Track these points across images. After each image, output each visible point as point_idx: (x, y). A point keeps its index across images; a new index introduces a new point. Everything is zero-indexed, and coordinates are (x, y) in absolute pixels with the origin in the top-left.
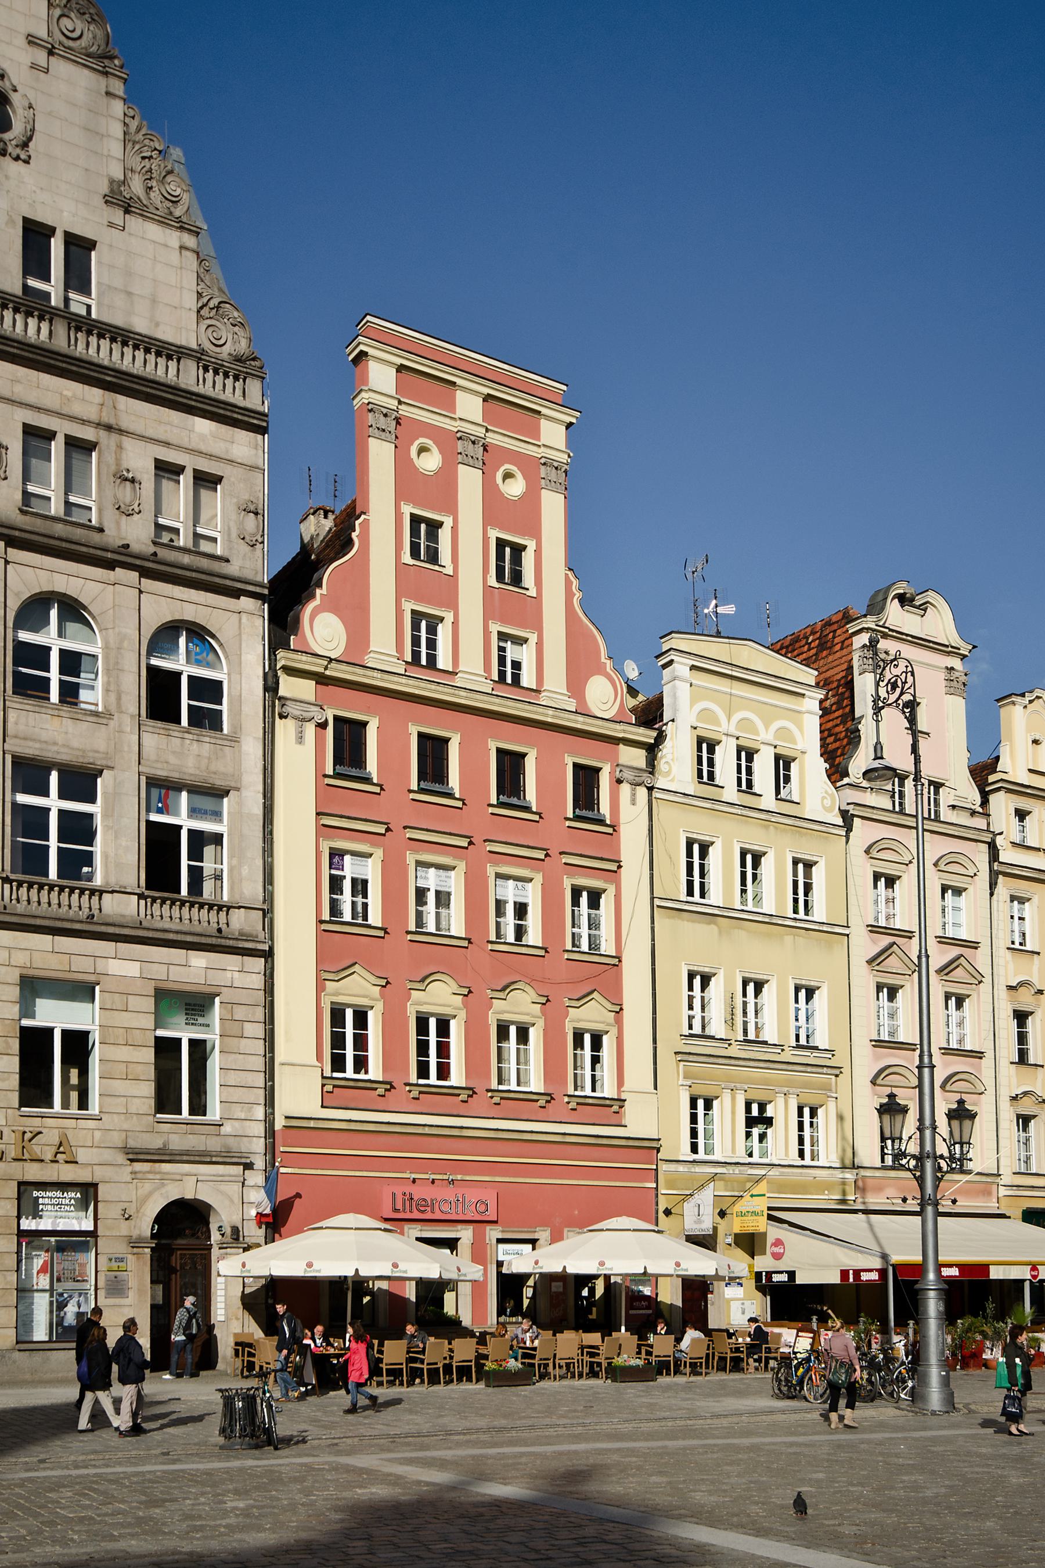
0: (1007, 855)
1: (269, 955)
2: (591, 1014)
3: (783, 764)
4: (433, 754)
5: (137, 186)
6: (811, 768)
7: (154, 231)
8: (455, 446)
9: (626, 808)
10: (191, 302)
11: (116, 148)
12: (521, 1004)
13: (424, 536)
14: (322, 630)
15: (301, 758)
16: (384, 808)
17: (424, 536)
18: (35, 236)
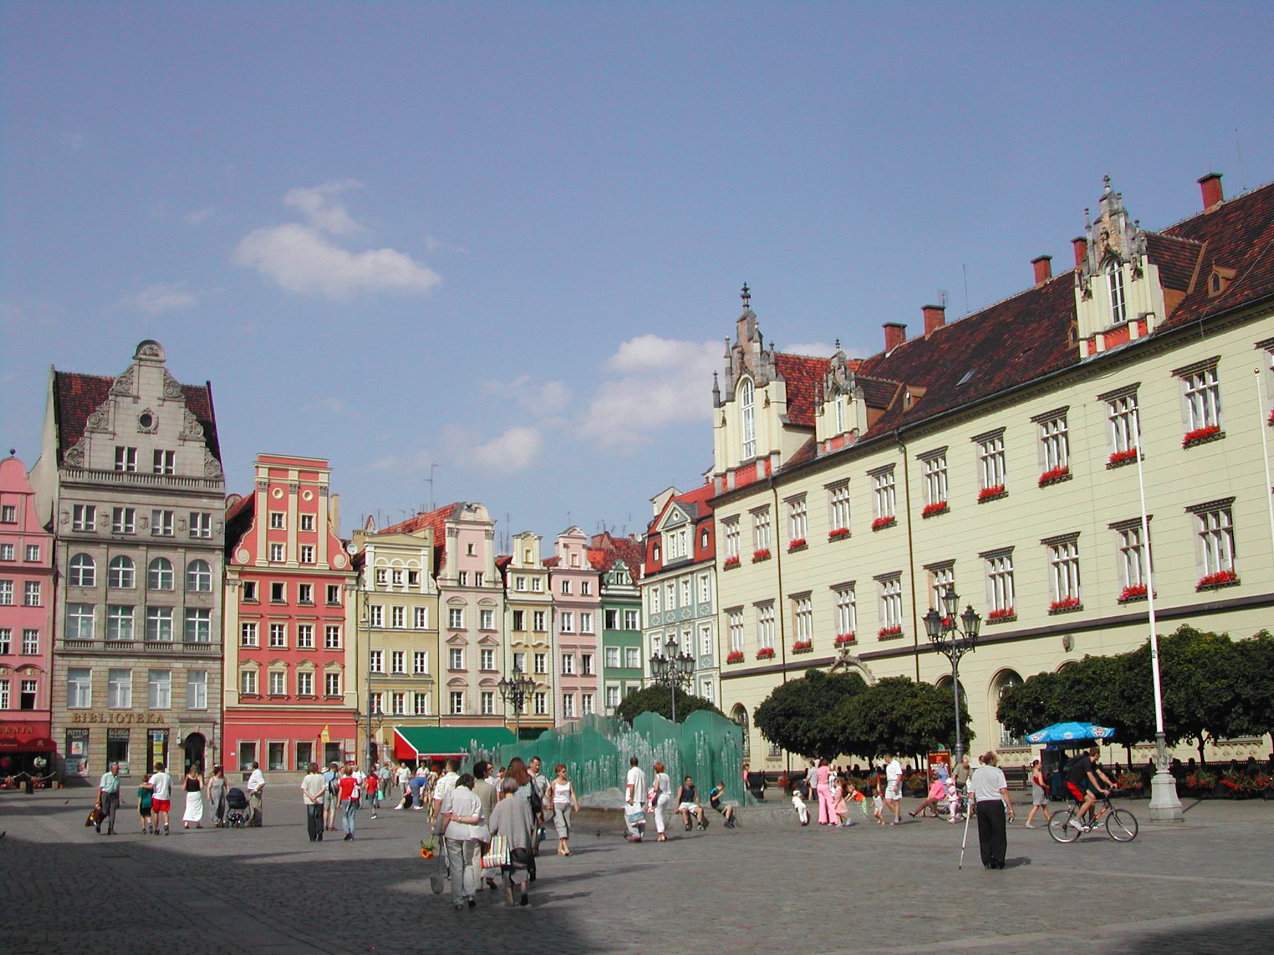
0: (511, 596)
1: (222, 659)
2: (334, 669)
3: (412, 576)
4: (277, 590)
5: (187, 432)
6: (424, 578)
7: (192, 443)
8: (289, 489)
9: (349, 600)
10: (203, 463)
11: (181, 422)
12: (308, 667)
13: (276, 518)
14: (241, 556)
15: (233, 596)
16: (261, 610)
17: (276, 518)
18: (157, 454)
